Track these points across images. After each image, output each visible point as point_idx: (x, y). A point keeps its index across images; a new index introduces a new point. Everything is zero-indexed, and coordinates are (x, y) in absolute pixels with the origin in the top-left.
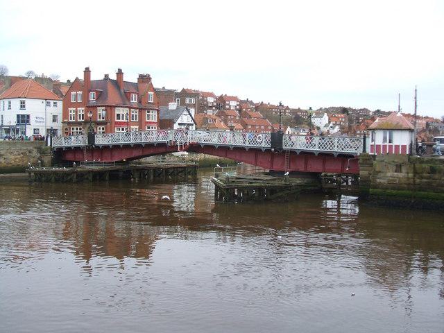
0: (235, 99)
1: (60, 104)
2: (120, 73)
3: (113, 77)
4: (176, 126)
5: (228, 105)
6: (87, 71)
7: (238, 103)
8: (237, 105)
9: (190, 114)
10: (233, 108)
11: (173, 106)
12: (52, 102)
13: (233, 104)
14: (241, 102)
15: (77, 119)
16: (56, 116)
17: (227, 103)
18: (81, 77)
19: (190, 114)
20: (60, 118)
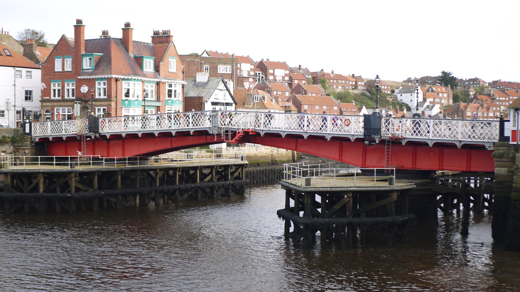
0: (283, 65)
1: (37, 74)
2: (127, 29)
3: (117, 34)
4: (208, 107)
5: (273, 74)
6: (79, 27)
7: (287, 72)
8: (286, 75)
9: (228, 90)
10: (278, 78)
11: (202, 77)
12: (24, 70)
13: (280, 73)
14: (292, 70)
15: (63, 96)
16: (31, 92)
17: (271, 71)
18: (71, 36)
19: (228, 90)
20: (37, 96)
